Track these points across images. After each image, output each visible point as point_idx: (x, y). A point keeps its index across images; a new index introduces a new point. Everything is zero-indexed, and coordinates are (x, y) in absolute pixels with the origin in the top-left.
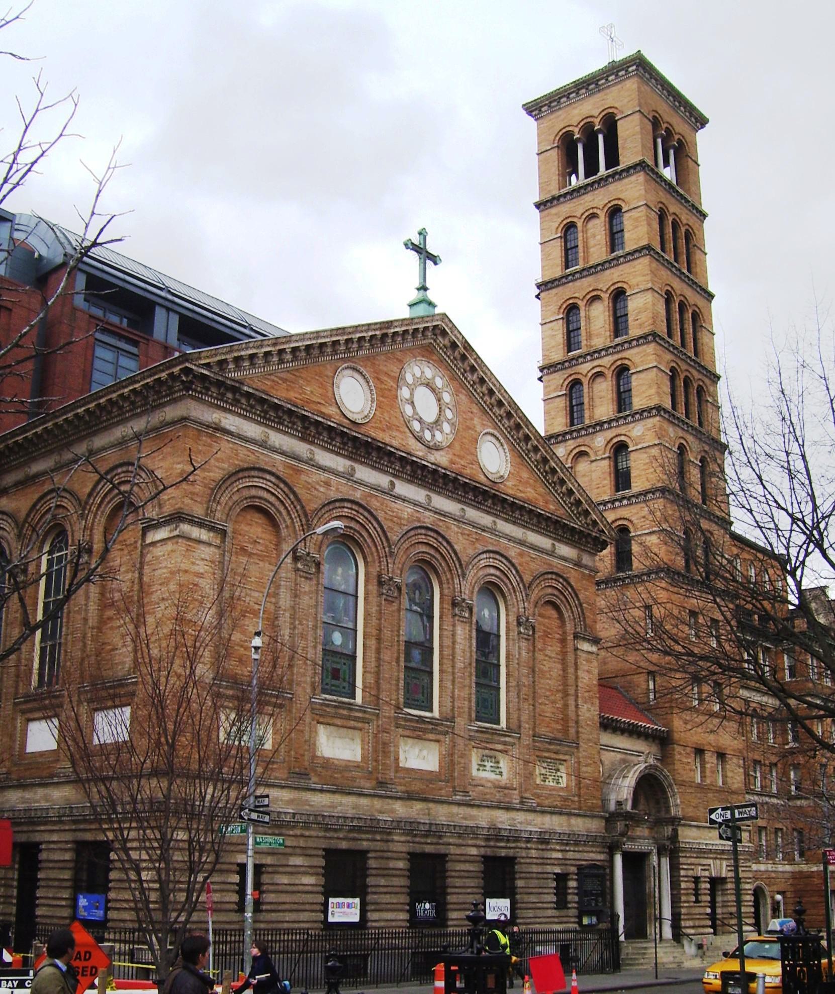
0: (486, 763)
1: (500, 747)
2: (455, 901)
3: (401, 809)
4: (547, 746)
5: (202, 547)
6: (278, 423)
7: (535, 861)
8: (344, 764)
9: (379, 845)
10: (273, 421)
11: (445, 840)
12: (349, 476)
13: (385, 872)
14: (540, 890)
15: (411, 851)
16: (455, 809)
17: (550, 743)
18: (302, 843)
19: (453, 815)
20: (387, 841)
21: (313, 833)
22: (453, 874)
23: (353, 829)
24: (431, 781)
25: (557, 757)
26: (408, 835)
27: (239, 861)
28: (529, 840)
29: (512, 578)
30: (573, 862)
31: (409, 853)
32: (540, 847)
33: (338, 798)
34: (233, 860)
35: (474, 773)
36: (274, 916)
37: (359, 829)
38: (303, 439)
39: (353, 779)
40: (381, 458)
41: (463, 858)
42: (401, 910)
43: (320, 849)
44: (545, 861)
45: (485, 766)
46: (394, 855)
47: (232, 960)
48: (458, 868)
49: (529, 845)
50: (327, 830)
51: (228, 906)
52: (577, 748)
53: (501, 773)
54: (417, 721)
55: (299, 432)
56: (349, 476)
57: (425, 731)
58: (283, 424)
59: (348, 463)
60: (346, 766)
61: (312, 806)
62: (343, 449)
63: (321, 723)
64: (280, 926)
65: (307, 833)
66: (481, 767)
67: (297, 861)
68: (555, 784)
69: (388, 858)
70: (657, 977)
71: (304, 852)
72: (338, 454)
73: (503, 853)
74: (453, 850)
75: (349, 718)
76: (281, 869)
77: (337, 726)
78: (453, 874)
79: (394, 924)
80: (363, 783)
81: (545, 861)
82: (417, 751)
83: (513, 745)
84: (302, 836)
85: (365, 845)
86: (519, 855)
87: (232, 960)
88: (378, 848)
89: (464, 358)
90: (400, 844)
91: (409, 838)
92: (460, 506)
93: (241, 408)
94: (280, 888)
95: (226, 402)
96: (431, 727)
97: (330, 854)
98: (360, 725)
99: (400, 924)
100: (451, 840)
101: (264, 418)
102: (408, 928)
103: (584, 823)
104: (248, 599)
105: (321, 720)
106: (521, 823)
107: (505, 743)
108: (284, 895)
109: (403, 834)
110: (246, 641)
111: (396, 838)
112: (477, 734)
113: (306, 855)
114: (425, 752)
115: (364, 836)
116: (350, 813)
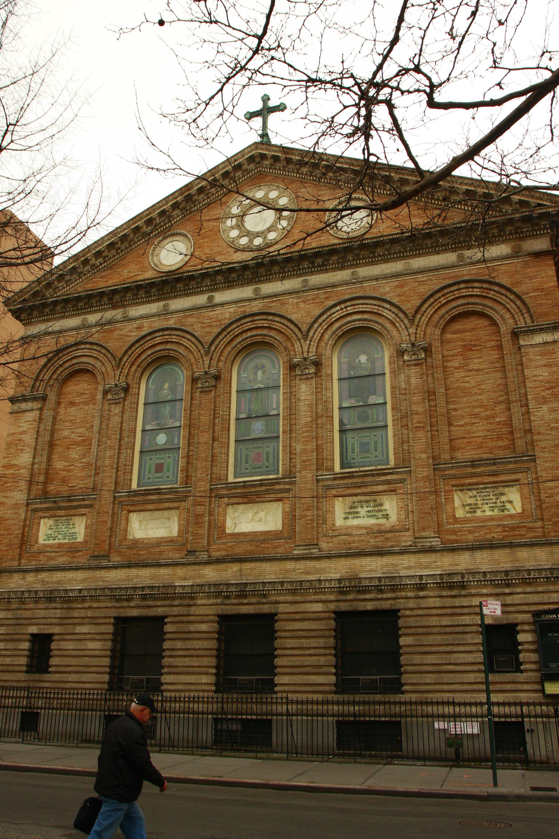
0: (359, 509)
1: (380, 488)
2: (285, 663)
3: (210, 574)
4: (469, 470)
5: (27, 414)
6: (90, 307)
7: (435, 612)
8: (155, 541)
9: (176, 611)
10: (85, 308)
11: (273, 599)
12: (166, 313)
13: (187, 636)
14: (449, 649)
15: (220, 613)
16: (290, 565)
17: (473, 466)
18: (89, 613)
19: (287, 571)
20: (190, 606)
21: (103, 605)
22: (284, 634)
23: (144, 597)
24: (263, 542)
25: (495, 479)
26: (216, 597)
27: (30, 632)
28: (421, 587)
29: (386, 313)
30: (526, 608)
31: (219, 616)
32: (444, 593)
33: (134, 572)
34: (24, 632)
35: (339, 522)
36: (63, 677)
37: (153, 597)
38: (114, 307)
39: (161, 553)
40: (188, 285)
41: (298, 616)
42: (207, 674)
43: (110, 617)
44: (459, 611)
45: (357, 513)
46: (198, 618)
47: (13, 712)
48: (290, 628)
49: (422, 594)
50: (117, 600)
51: (17, 668)
52: (534, 461)
53: (387, 516)
54: (244, 487)
55: (109, 304)
56: (166, 313)
57: (259, 494)
58: (92, 307)
59: (161, 304)
60: (157, 543)
61: (106, 581)
62: (151, 296)
63: (133, 511)
64: (63, 685)
65: (96, 605)
66: (352, 513)
67: (85, 629)
68: (496, 512)
69: (190, 622)
70: (495, 784)
71: (93, 621)
72: (150, 302)
73: (386, 605)
74: (282, 608)
75: (160, 501)
76: (68, 637)
77: (151, 510)
78: (284, 634)
79: (193, 687)
80: (171, 555)
81: (459, 611)
82: (250, 515)
83: (402, 481)
84: (90, 608)
85: (160, 611)
86: (401, 606)
87: (13, 712)
88: (176, 613)
89: (289, 161)
90: (207, 607)
91: (219, 601)
92: (300, 279)
93: (60, 313)
94: (65, 653)
95: (47, 315)
96: (264, 488)
97: (121, 622)
98: (175, 505)
99: (205, 687)
100: (282, 598)
101: (78, 310)
102: (215, 692)
103: (552, 553)
104: (73, 436)
105: (132, 508)
106: (409, 568)
107: (388, 482)
108: (69, 659)
109: (209, 597)
110: (70, 466)
111: (200, 602)
112: (336, 482)
113: (96, 624)
114: (262, 514)
115: (159, 603)
116: (148, 582)
